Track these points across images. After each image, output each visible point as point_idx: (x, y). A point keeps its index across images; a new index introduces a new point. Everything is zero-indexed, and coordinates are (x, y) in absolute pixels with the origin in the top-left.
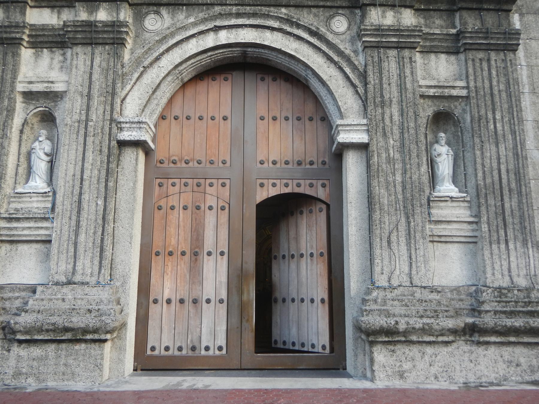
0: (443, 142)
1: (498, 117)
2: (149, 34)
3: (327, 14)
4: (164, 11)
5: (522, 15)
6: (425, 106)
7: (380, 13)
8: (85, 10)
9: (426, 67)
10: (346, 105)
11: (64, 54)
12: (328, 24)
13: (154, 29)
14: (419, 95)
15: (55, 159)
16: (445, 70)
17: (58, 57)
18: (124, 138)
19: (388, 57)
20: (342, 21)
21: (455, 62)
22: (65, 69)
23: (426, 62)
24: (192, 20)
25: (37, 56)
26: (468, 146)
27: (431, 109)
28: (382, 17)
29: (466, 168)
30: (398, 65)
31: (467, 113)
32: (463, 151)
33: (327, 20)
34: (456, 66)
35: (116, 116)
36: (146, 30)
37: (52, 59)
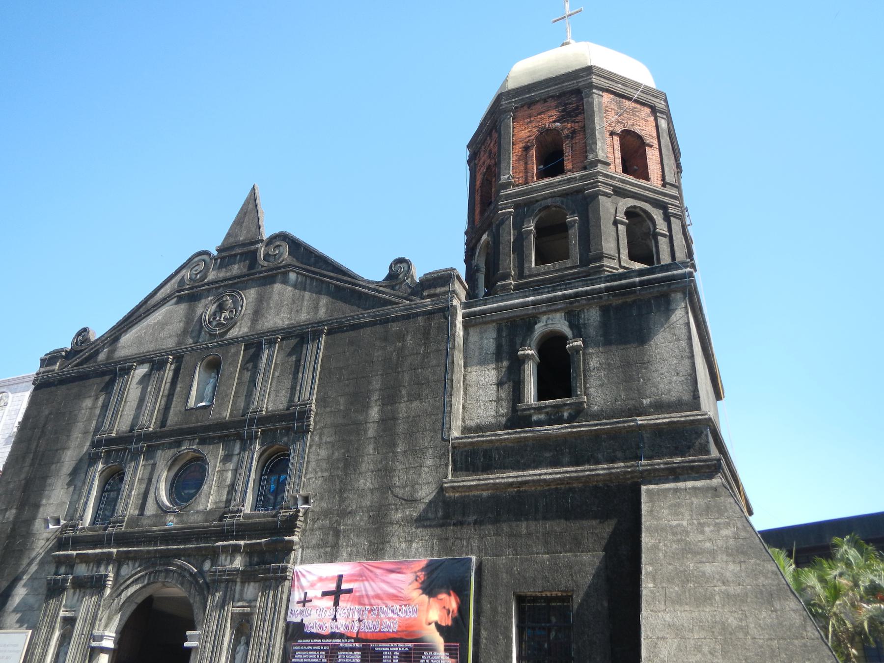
1: (266, 626)
4: (130, 563)
5: (303, 550)
25: (74, 593)
37: (79, 595)
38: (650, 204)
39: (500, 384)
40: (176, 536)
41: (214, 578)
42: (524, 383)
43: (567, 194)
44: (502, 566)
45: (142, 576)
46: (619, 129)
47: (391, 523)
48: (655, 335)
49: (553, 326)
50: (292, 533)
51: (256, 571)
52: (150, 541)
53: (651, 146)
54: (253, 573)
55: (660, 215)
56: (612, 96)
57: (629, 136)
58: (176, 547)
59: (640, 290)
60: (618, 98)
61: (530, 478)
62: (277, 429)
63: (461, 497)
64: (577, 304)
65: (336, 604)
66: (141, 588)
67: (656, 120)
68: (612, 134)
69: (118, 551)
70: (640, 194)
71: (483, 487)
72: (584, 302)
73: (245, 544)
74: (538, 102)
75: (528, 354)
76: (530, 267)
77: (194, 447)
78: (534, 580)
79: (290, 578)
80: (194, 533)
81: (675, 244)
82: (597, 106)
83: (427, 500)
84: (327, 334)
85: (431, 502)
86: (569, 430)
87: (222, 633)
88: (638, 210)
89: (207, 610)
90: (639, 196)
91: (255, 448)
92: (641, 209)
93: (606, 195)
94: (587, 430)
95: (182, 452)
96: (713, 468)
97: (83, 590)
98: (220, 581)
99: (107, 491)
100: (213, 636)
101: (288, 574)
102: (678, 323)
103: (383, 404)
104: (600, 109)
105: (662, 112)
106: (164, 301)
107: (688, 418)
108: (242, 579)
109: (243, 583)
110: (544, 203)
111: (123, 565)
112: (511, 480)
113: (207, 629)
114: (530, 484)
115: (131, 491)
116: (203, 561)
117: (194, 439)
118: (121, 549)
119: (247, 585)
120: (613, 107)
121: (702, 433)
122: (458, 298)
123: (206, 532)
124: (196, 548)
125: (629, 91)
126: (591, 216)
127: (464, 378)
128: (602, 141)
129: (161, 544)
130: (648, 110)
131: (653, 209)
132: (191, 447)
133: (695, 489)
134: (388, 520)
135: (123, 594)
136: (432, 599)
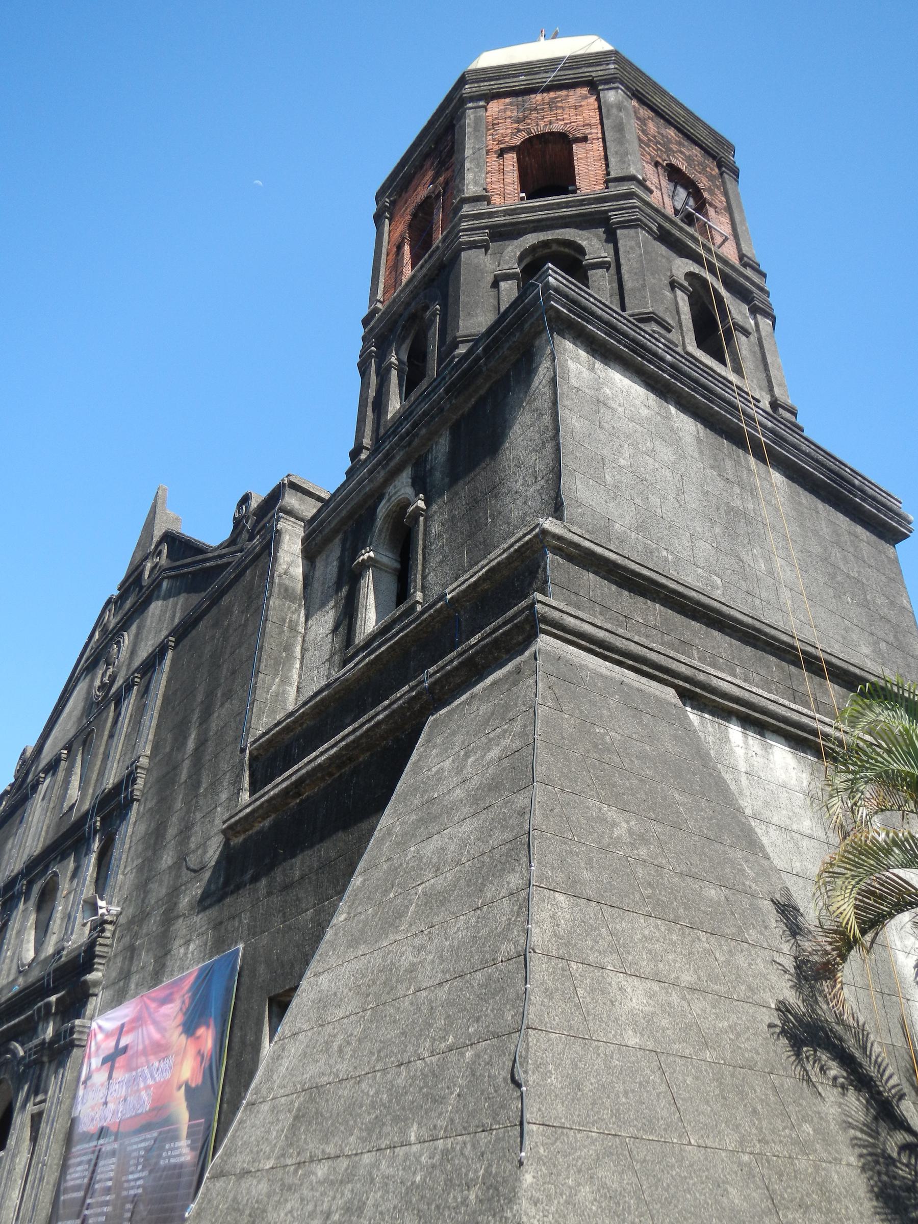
38: (577, 227)
39: (335, 630)
42: (357, 611)
43: (432, 280)
44: (261, 950)
46: (517, 141)
47: (178, 917)
48: (510, 427)
49: (399, 493)
50: (90, 968)
53: (585, 139)
55: (598, 237)
56: (508, 100)
57: (550, 146)
59: (485, 364)
60: (520, 99)
61: (304, 771)
63: (245, 841)
64: (416, 441)
65: (110, 1077)
67: (598, 99)
68: (501, 153)
70: (547, 219)
71: (261, 811)
72: (424, 431)
73: (58, 1000)
74: (415, 173)
75: (363, 560)
76: (386, 421)
78: (292, 965)
79: (83, 1043)
81: (624, 269)
82: (473, 125)
83: (213, 863)
84: (175, 648)
85: (218, 863)
86: (367, 660)
88: (555, 247)
90: (548, 223)
92: (557, 241)
93: (473, 245)
94: (387, 649)
96: (528, 627)
101: (75, 1036)
102: (541, 387)
103: (200, 724)
104: (476, 129)
105: (607, 82)
106: (78, 679)
107: (512, 549)
110: (406, 314)
112: (284, 785)
114: (307, 782)
120: (508, 114)
121: (539, 566)
122: (297, 518)
125: (537, 79)
126: (451, 289)
127: (304, 641)
128: (476, 170)
130: (584, 91)
131: (580, 232)
133: (494, 683)
134: (175, 913)
136: (189, 1040)
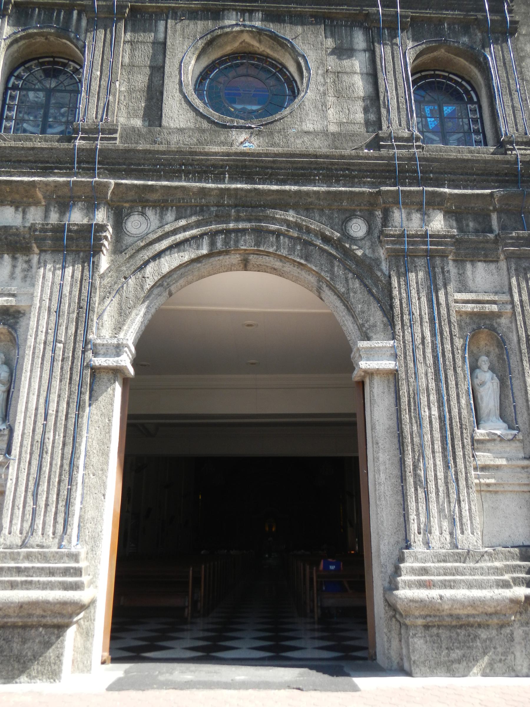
0: (485, 367)
2: (131, 239)
3: (344, 217)
4: (150, 213)
6: (463, 324)
7: (404, 215)
8: (56, 209)
9: (462, 278)
10: (368, 323)
11: (28, 262)
12: (343, 227)
13: (138, 233)
14: (454, 311)
15: (14, 389)
16: (484, 281)
17: (22, 266)
18: (100, 363)
19: (415, 267)
20: (360, 224)
21: (494, 271)
22: (30, 279)
23: (461, 272)
24: (183, 222)
26: (517, 371)
27: (470, 327)
28: (408, 220)
29: (515, 399)
30: (428, 276)
31: (512, 332)
32: (511, 378)
33: (343, 223)
34: (496, 276)
35: (91, 337)
36: (128, 233)
37: (14, 267)
40: (272, 168)
41: (398, 247)
45: (194, 238)
51: (487, 242)
52: (205, 172)
54: (481, 245)
58: (275, 187)
62: (441, 21)
66: (192, 261)
69: (117, 185)
77: (258, 24)
80: (319, 167)
87: (448, 347)
89: (397, 302)
91: (404, 45)
95: (228, 30)
97: (21, 259)
98: (413, 255)
99: (15, 88)
100: (429, 350)
108: (457, 254)
109: (460, 262)
111: (129, 215)
113: (408, 337)
115: (111, 82)
116: (348, 219)
117: (251, 12)
118: (124, 181)
119: (469, 266)
123: (348, 167)
124: (329, 192)
129: (233, 180)
132: (247, 23)
135: (149, 269)
